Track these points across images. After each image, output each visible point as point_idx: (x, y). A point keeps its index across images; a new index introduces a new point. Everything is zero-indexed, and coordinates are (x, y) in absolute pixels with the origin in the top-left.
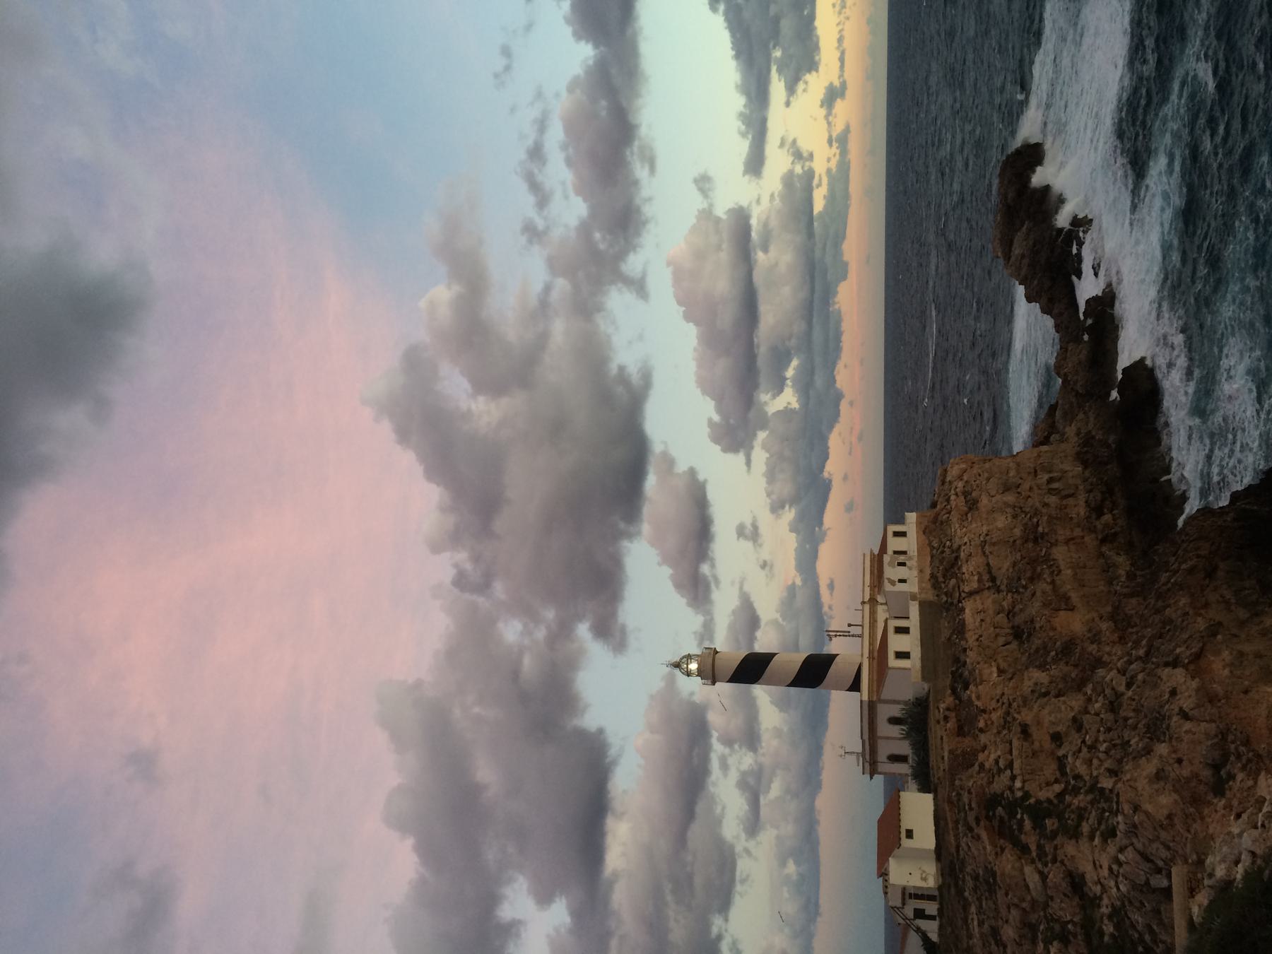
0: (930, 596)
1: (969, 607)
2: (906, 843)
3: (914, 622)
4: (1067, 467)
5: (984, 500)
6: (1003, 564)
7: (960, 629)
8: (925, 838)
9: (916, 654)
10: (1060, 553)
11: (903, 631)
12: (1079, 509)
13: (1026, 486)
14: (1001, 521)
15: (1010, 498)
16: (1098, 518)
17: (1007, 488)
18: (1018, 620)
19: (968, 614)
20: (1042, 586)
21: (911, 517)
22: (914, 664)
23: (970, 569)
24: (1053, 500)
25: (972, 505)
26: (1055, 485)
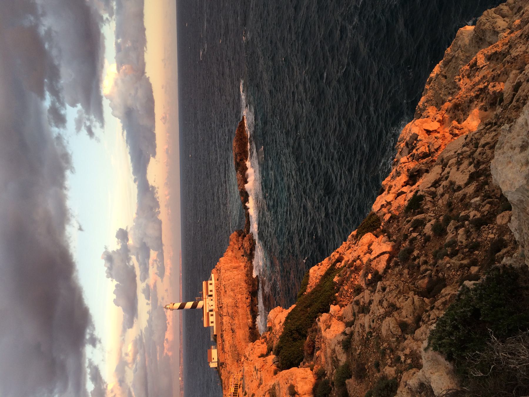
0: (217, 310)
1: (224, 318)
2: (213, 361)
3: (214, 313)
4: (243, 284)
5: (228, 292)
6: (230, 311)
7: (223, 324)
8: (216, 360)
9: (215, 322)
10: (240, 311)
11: (212, 315)
12: (244, 299)
13: (236, 291)
14: (231, 300)
15: (232, 294)
16: (247, 299)
17: (232, 290)
18: (233, 327)
19: (224, 321)
20: (236, 322)
21: (213, 275)
22: (214, 325)
23: (225, 310)
24: (240, 296)
25: (226, 291)
26: (241, 290)
